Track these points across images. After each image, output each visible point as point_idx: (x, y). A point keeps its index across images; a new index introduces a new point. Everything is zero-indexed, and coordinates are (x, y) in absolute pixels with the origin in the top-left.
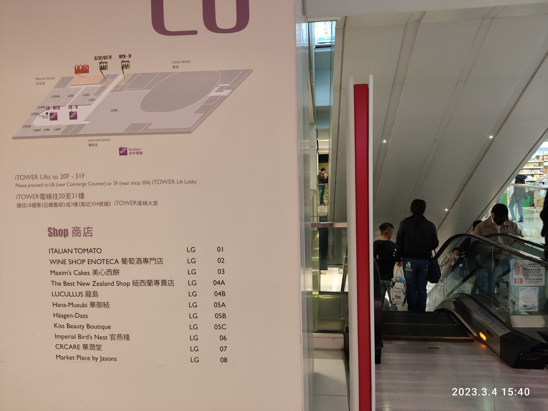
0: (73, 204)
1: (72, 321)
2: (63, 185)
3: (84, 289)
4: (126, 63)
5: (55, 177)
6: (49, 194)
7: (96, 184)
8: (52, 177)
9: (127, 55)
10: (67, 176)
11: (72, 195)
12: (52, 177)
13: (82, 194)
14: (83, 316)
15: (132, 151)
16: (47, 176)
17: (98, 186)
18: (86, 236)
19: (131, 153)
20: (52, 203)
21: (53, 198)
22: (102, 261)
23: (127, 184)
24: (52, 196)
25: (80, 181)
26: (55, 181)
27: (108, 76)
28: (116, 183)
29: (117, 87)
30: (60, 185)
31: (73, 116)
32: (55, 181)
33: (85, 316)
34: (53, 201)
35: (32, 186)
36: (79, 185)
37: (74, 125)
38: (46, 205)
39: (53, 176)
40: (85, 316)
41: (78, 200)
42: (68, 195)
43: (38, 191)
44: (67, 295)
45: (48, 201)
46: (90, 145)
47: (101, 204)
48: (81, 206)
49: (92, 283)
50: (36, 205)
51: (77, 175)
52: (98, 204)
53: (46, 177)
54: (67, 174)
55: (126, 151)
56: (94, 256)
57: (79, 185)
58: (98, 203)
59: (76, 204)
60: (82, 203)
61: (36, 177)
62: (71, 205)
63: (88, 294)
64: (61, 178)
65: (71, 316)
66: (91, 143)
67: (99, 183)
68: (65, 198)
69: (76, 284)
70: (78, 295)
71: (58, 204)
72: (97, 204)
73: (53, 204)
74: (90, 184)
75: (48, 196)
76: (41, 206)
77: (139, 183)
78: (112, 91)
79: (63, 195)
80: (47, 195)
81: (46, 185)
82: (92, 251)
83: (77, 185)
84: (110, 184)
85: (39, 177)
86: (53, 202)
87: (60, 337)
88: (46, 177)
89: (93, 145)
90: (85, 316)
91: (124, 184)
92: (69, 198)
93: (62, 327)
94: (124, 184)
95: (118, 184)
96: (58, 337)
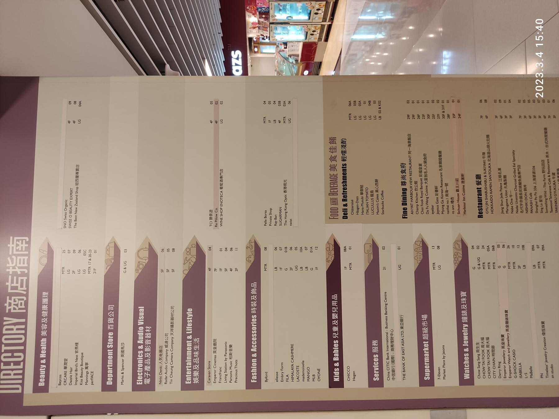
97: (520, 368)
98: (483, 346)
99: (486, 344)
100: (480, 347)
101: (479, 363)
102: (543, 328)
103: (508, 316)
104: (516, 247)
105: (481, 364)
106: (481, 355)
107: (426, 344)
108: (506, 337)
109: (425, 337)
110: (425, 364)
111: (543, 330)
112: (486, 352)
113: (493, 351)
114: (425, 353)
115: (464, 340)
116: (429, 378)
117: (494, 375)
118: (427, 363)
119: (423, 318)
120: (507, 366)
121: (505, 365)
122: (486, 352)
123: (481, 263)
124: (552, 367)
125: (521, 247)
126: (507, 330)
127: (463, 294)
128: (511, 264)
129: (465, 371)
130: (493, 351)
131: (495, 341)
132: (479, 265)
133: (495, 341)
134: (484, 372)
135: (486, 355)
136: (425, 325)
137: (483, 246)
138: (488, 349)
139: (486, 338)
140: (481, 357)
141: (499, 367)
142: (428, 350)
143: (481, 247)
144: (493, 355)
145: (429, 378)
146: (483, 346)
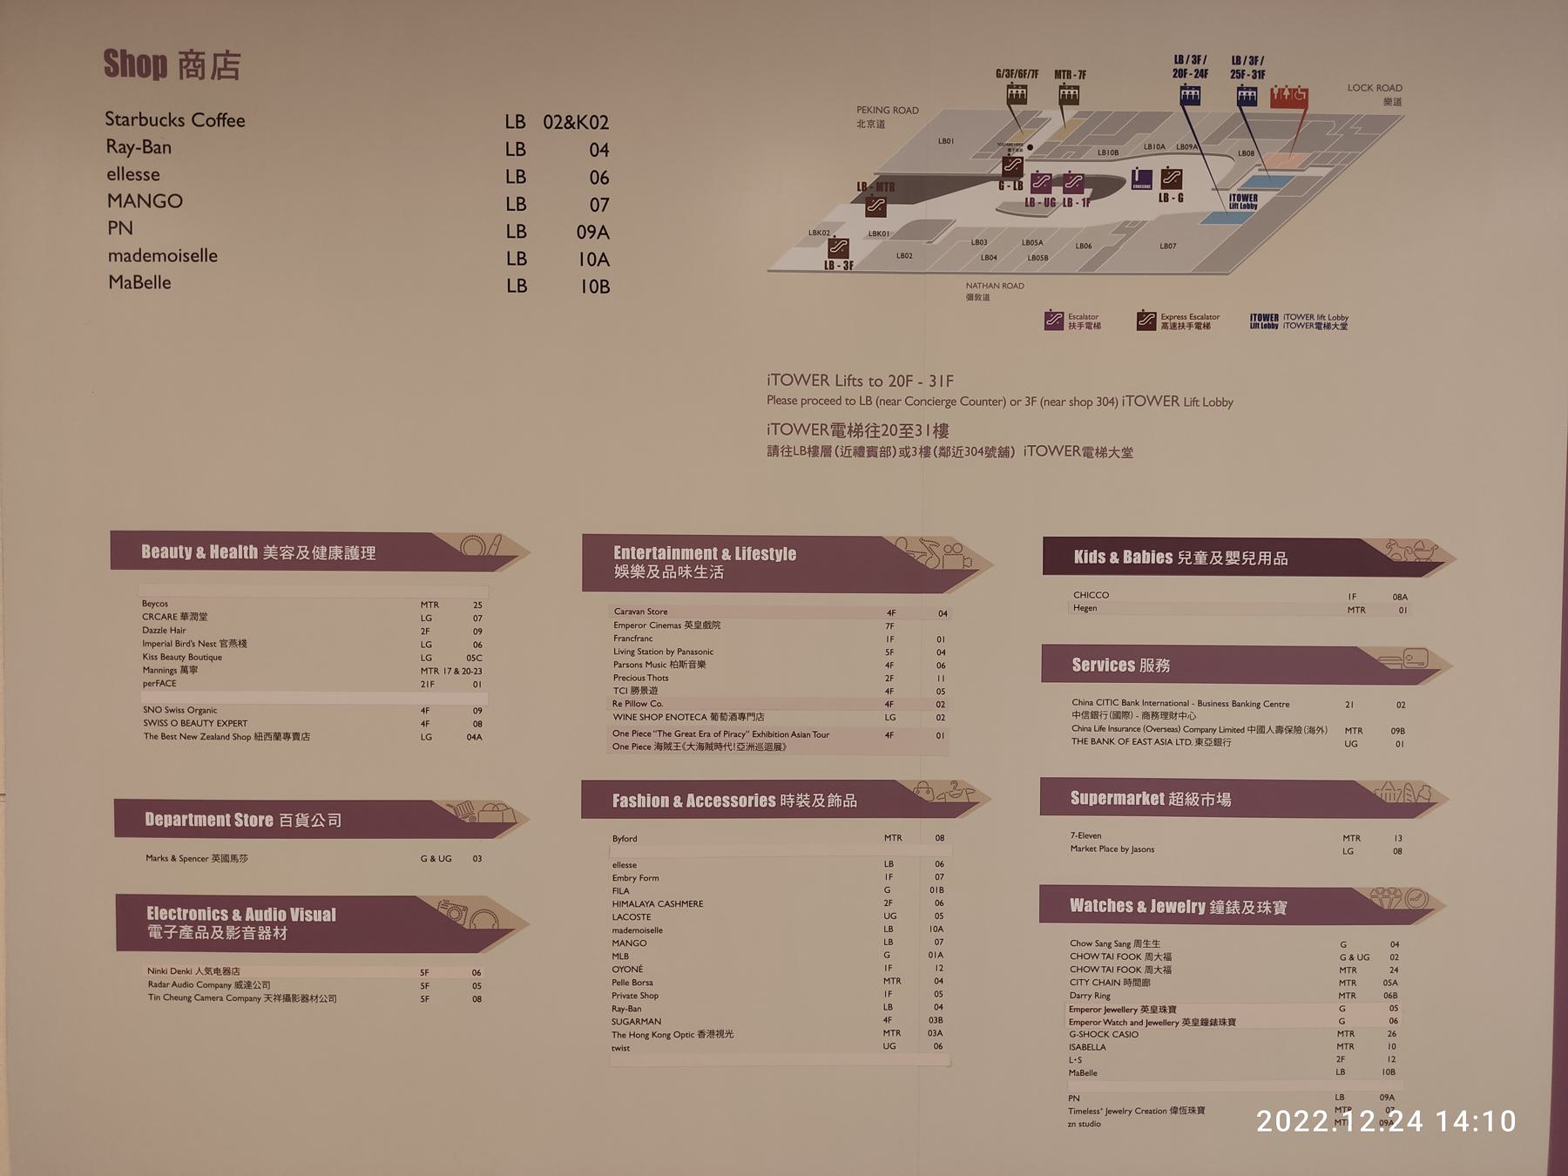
0: (918, 451)
2: (896, 403)
5: (876, 382)
6: (856, 425)
7: (982, 402)
8: (866, 382)
9: (1075, 72)
10: (907, 380)
11: (916, 429)
12: (866, 382)
13: (944, 427)
15: (1076, 321)
16: (854, 379)
17: (985, 407)
19: (1072, 326)
20: (862, 448)
21: (865, 434)
23: (1060, 403)
25: (940, 393)
26: (875, 392)
28: (1031, 401)
30: (887, 402)
32: (875, 392)
34: (865, 442)
35: (810, 401)
36: (936, 402)
39: (871, 379)
42: (906, 430)
43: (830, 415)
45: (853, 442)
46: (970, 297)
47: (990, 452)
48: (938, 456)
50: (820, 452)
51: (933, 378)
52: (982, 453)
53: (851, 381)
54: (908, 376)
55: (1062, 320)
57: (936, 402)
58: (982, 449)
59: (926, 451)
60: (942, 448)
61: (824, 379)
62: (912, 452)
64: (891, 386)
66: (974, 291)
67: (990, 400)
68: (899, 434)
71: (879, 450)
72: (981, 451)
74: (965, 401)
75: (853, 429)
76: (833, 454)
77: (1090, 403)
79: (894, 427)
80: (850, 427)
81: (850, 402)
83: (931, 402)
84: (1017, 402)
85: (832, 380)
88: (851, 381)
89: (978, 297)
91: (1052, 403)
92: (908, 435)
94: (1052, 403)
95: (1037, 404)
97: (1094, 1048)
98: (1149, 956)
99: (1154, 964)
100: (1148, 950)
101: (1109, 946)
102: (1187, 1109)
103: (1220, 1026)
104: (1392, 1053)
105: (1105, 949)
106: (1129, 952)
107: (1157, 799)
108: (1169, 1017)
109: (1176, 799)
110: (1109, 794)
111: (1183, 1109)
112: (1136, 963)
113: (1137, 982)
114: (1137, 795)
115: (1167, 903)
116: (1075, 802)
117: (1079, 981)
118: (1112, 799)
119: (1221, 795)
120: (1100, 1016)
121: (1102, 1011)
122: (1136, 963)
123: (1354, 963)
124: (1093, 1124)
125: (1391, 1066)
126: (1186, 1022)
127: (1281, 908)
128: (1349, 1040)
129: (1090, 902)
130: (1137, 982)
131: (1160, 990)
132: (1352, 958)
133: (1160, 990)
134: (1087, 956)
135: (1129, 963)
136: (1205, 800)
137: (1397, 970)
138: (1143, 970)
139: (1170, 967)
140: (1123, 950)
141: (1096, 995)
142: (1144, 803)
143: (1395, 964)
144: (1127, 982)
145: (1075, 802)
146: (1149, 956)
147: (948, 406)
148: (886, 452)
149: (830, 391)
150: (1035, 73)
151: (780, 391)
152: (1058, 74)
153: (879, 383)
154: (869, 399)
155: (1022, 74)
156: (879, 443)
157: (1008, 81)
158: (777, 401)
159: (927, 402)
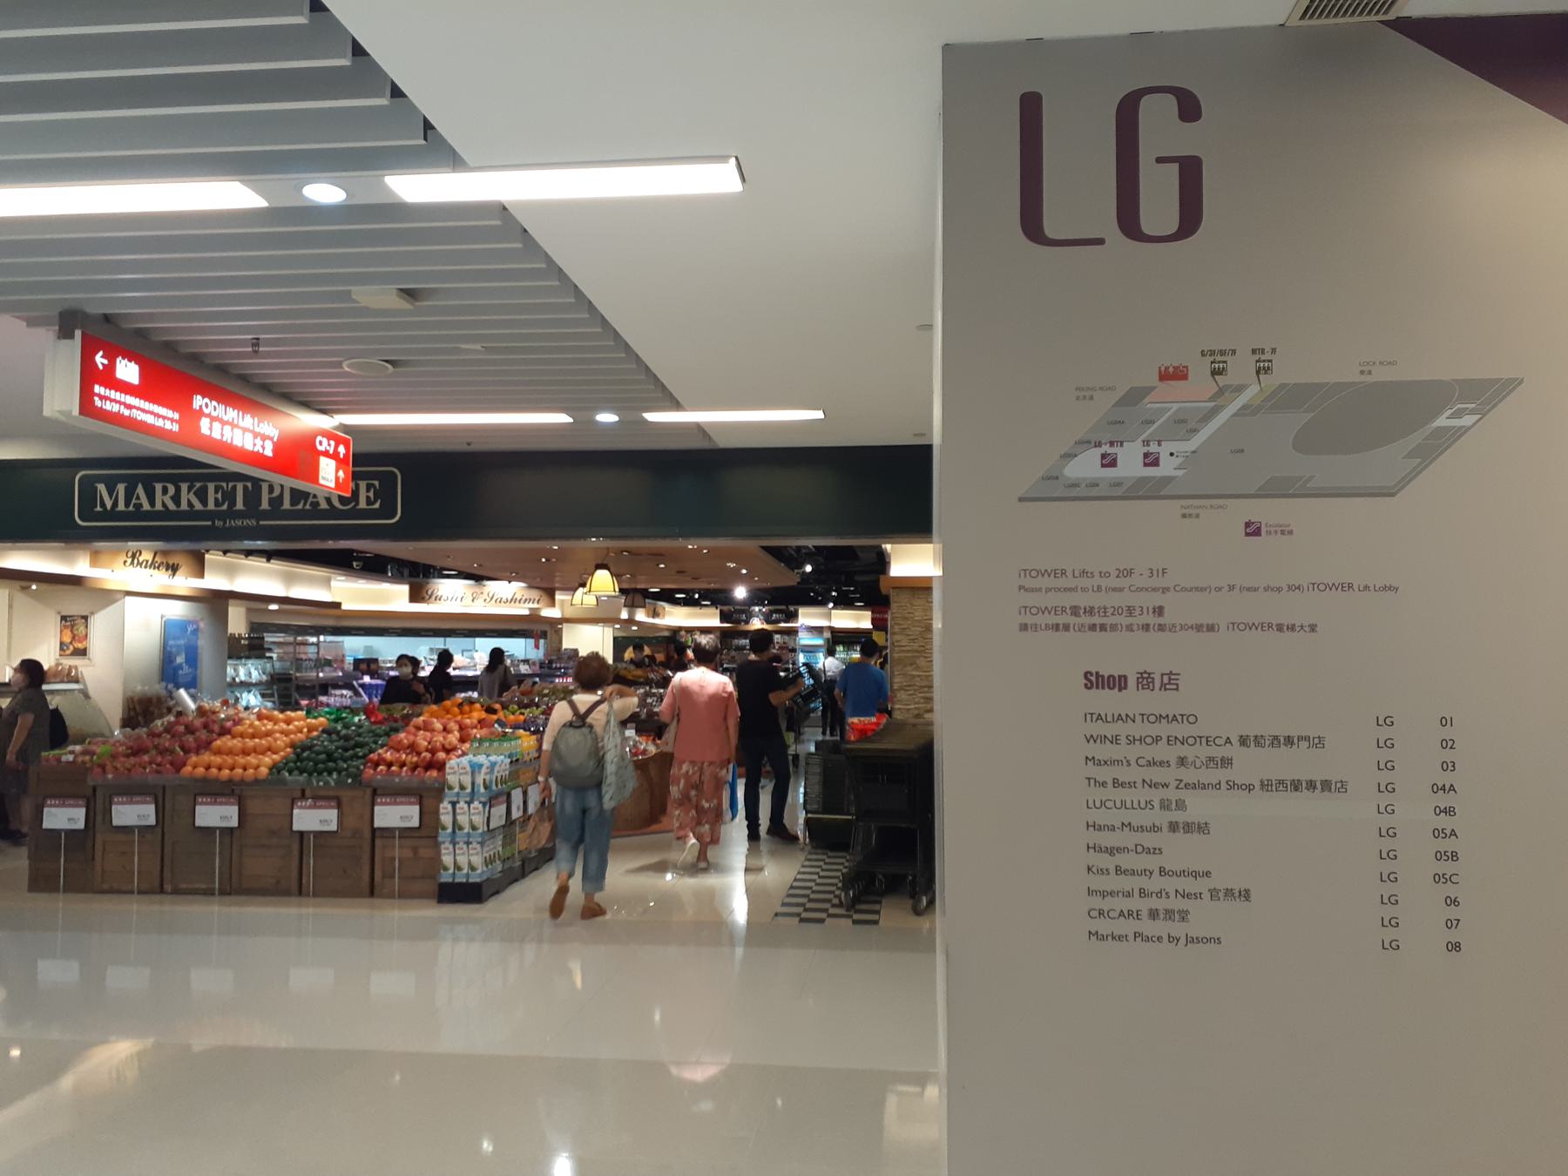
1: (1125, 861)
2: (1121, 590)
3: (1156, 795)
4: (1266, 364)
5: (1106, 575)
10: (1130, 572)
14: (1152, 851)
18: (1165, 689)
19: (1269, 533)
20: (1094, 625)
21: (1097, 614)
22: (1198, 739)
23: (1256, 590)
24: (1096, 610)
26: (1104, 583)
27: (1227, 387)
28: (1232, 588)
29: (1244, 407)
30: (1114, 590)
31: (1151, 461)
32: (1104, 583)
33: (1157, 851)
36: (1154, 590)
37: (1154, 478)
38: (1081, 628)
39: (1101, 573)
40: (1157, 851)
41: (1152, 620)
43: (1068, 600)
44: (1118, 805)
49: (1173, 784)
55: (1259, 529)
56: (1180, 730)
57: (1154, 590)
63: (1165, 805)
64: (1117, 577)
65: (1126, 850)
68: (1124, 614)
69: (1139, 785)
70: (1143, 805)
72: (1192, 627)
73: (1098, 626)
78: (1235, 415)
80: (1085, 609)
81: (1084, 590)
82: (1177, 720)
84: (1220, 589)
86: (1097, 623)
87: (1098, 894)
90: (1157, 851)
91: (1248, 589)
93: (1103, 872)
94: (1248, 589)
95: (1237, 590)
96: (1094, 893)
147: (1163, 592)
148: (1114, 627)
149: (1071, 583)
150: (1234, 352)
151: (1029, 583)
152: (1254, 351)
153: (1107, 575)
154: (1099, 588)
155: (1222, 353)
156: (1108, 621)
157: (1212, 359)
158: (1026, 590)
159: (1147, 590)
